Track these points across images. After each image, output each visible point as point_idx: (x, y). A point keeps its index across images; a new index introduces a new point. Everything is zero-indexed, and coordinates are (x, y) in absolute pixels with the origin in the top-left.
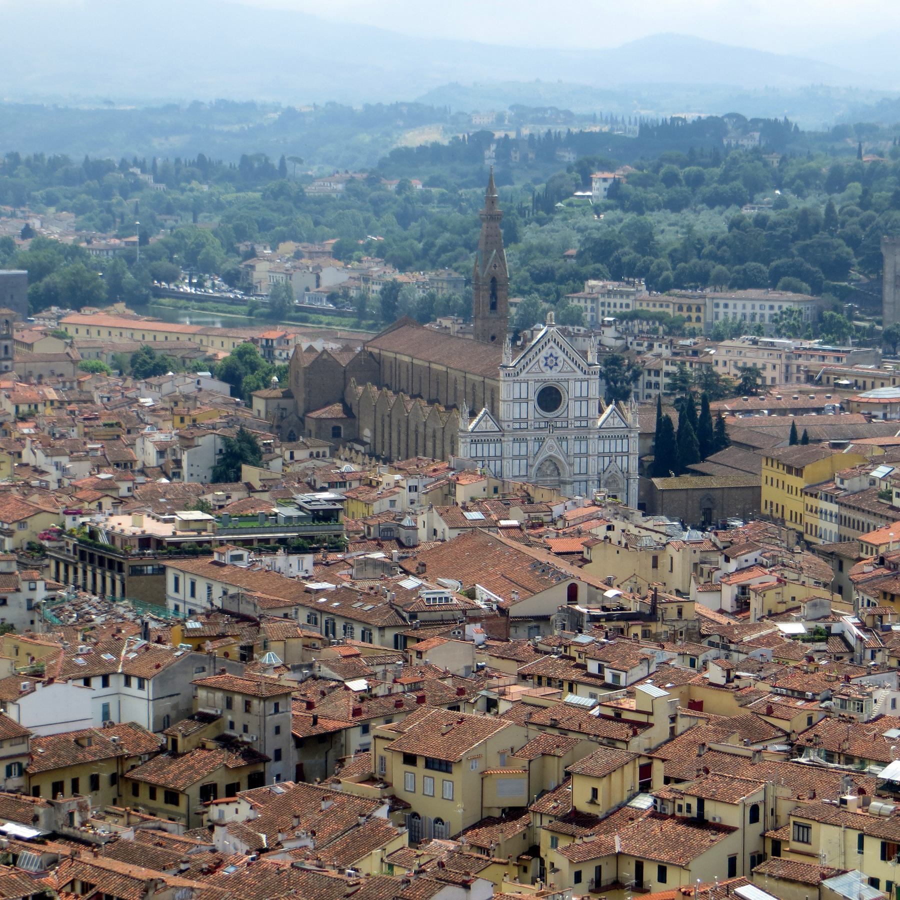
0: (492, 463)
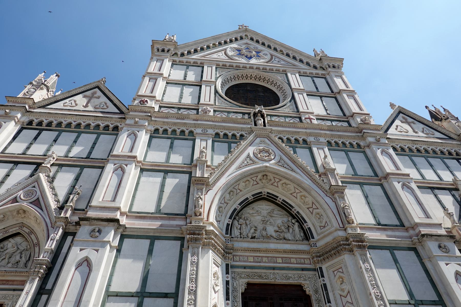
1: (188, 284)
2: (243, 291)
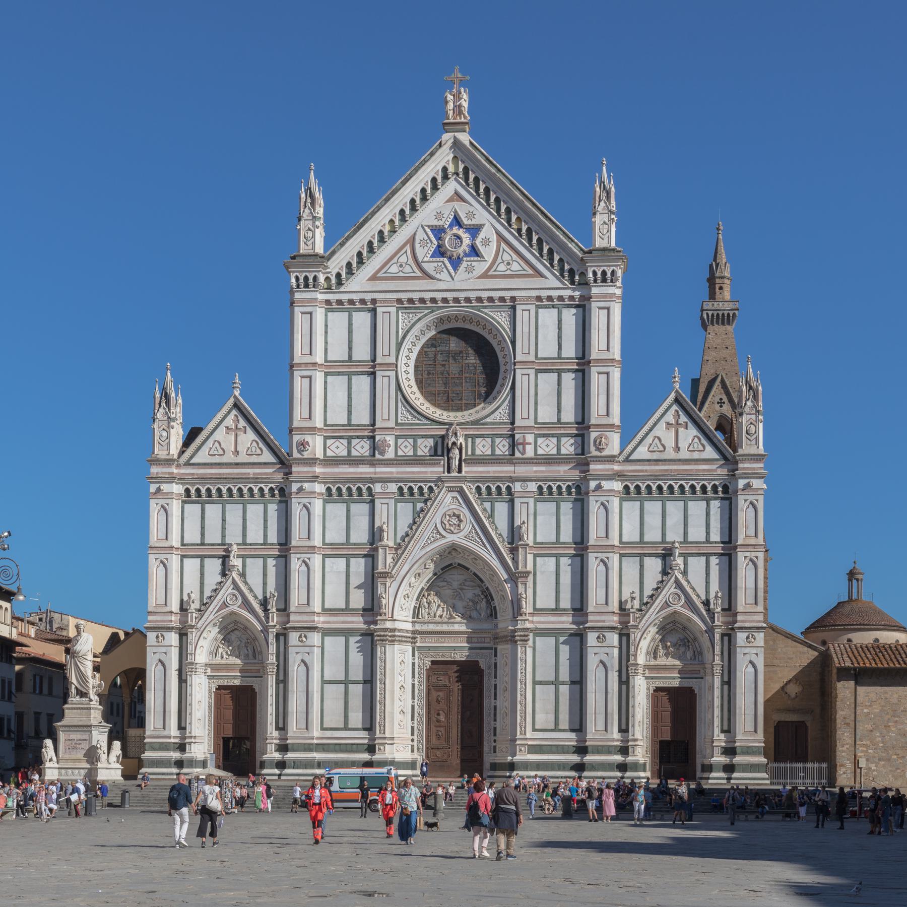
1: (378, 677)
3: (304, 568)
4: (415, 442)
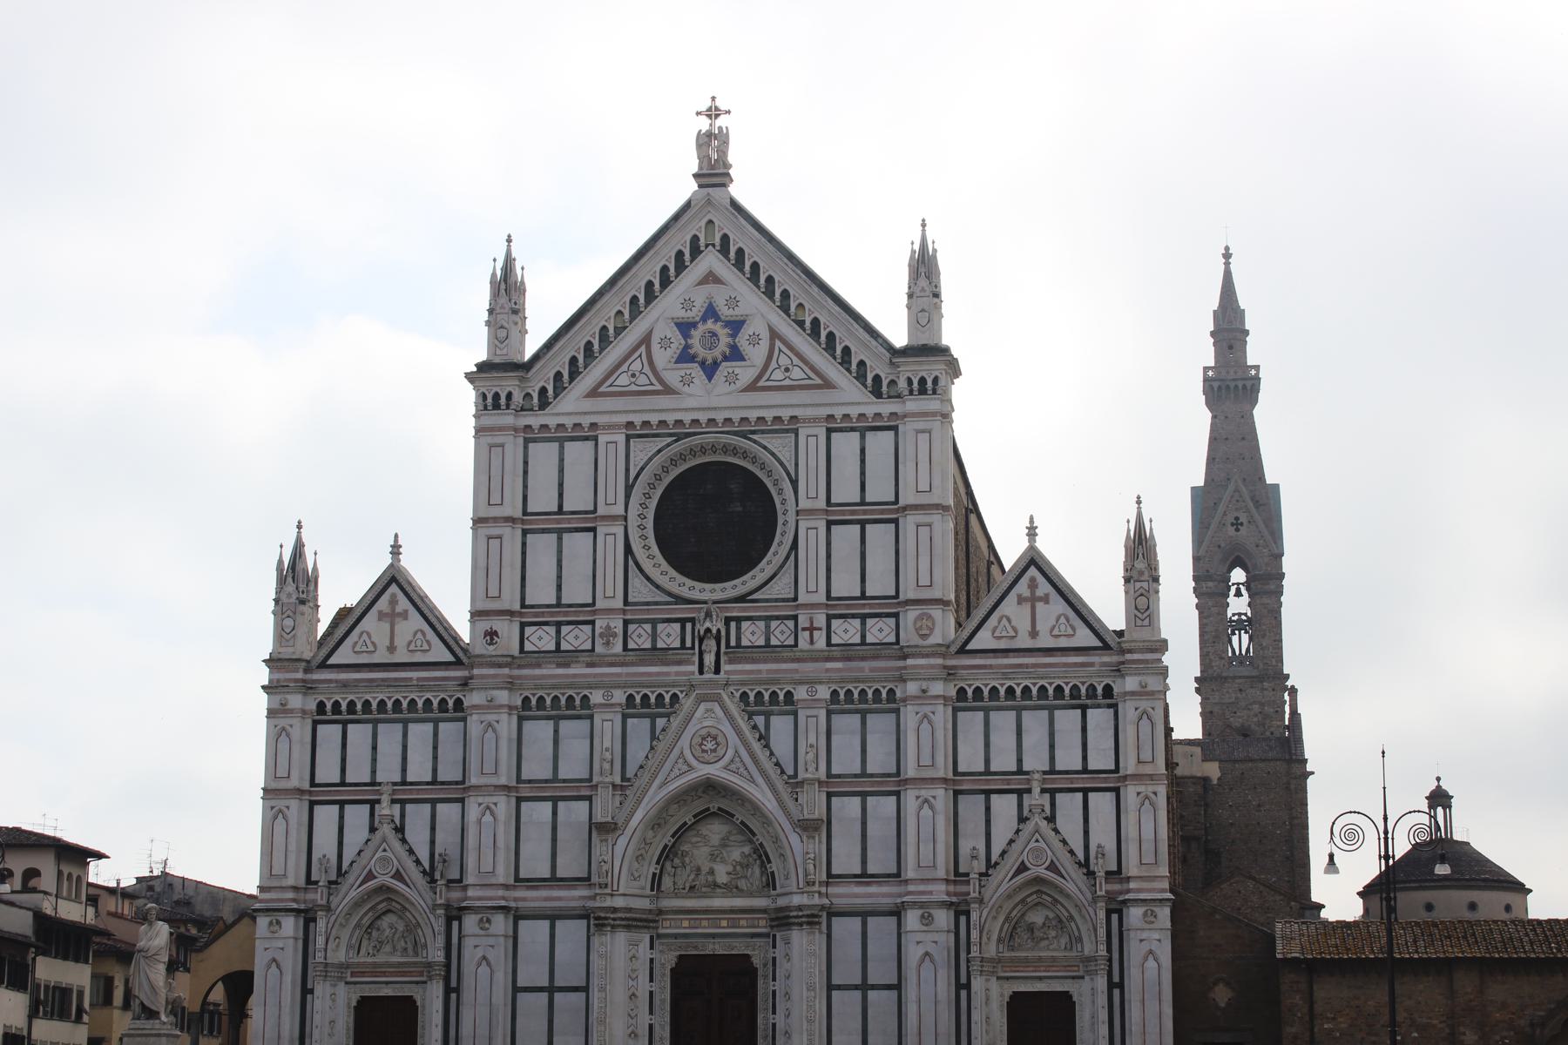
0: (417, 817)
2: (674, 965)
3: (488, 818)
4: (654, 629)
